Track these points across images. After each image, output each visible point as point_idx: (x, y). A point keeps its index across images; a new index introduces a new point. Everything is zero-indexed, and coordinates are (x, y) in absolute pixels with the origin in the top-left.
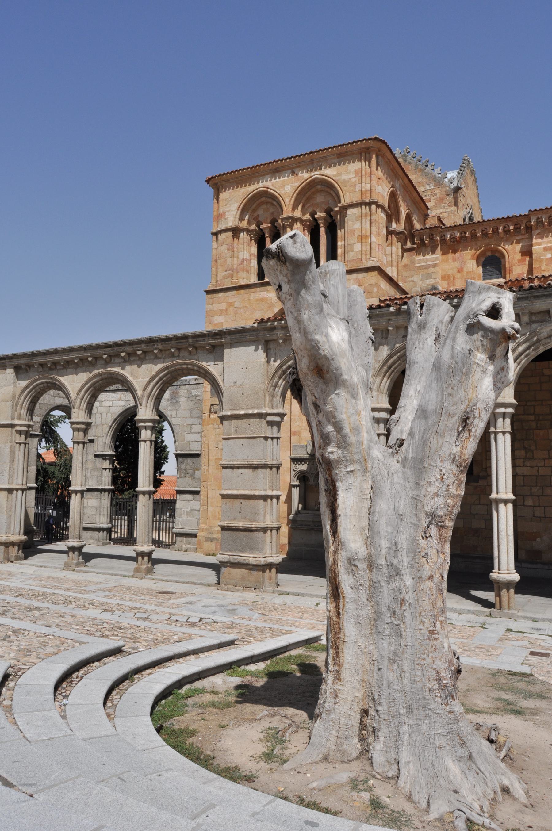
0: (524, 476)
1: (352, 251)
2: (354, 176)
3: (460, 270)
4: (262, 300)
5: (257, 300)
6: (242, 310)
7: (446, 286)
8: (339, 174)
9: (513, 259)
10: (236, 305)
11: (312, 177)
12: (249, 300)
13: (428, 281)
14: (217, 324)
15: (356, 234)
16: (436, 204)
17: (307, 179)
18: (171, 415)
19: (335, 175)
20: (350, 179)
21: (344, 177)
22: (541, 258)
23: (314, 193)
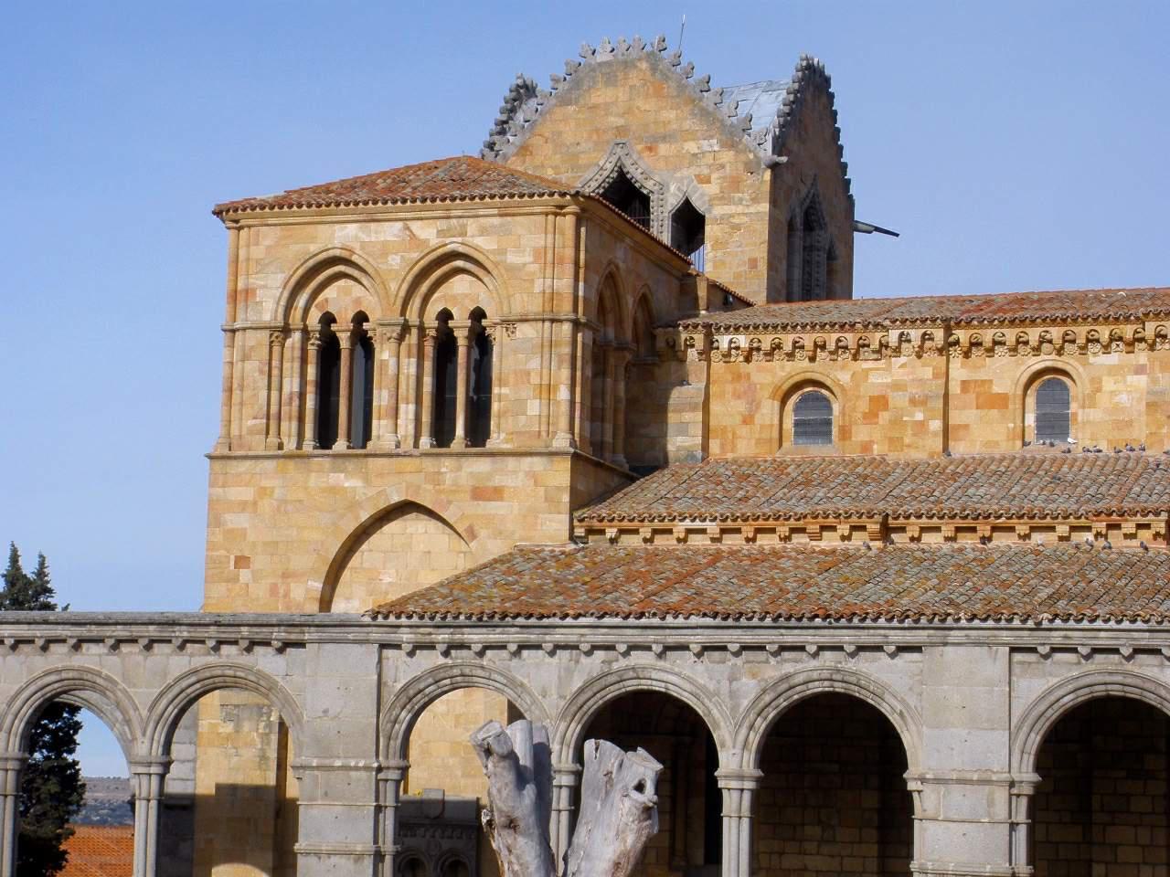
0: (817, 872)
1: (524, 413)
2: (531, 259)
3: (747, 420)
4: (334, 490)
6: (290, 507)
7: (718, 452)
8: (502, 251)
9: (854, 410)
10: (277, 494)
11: (446, 245)
12: (306, 488)
13: (679, 439)
15: (532, 381)
16: (722, 192)
17: (437, 249)
19: (493, 252)
20: (524, 265)
21: (512, 258)
22: (905, 419)
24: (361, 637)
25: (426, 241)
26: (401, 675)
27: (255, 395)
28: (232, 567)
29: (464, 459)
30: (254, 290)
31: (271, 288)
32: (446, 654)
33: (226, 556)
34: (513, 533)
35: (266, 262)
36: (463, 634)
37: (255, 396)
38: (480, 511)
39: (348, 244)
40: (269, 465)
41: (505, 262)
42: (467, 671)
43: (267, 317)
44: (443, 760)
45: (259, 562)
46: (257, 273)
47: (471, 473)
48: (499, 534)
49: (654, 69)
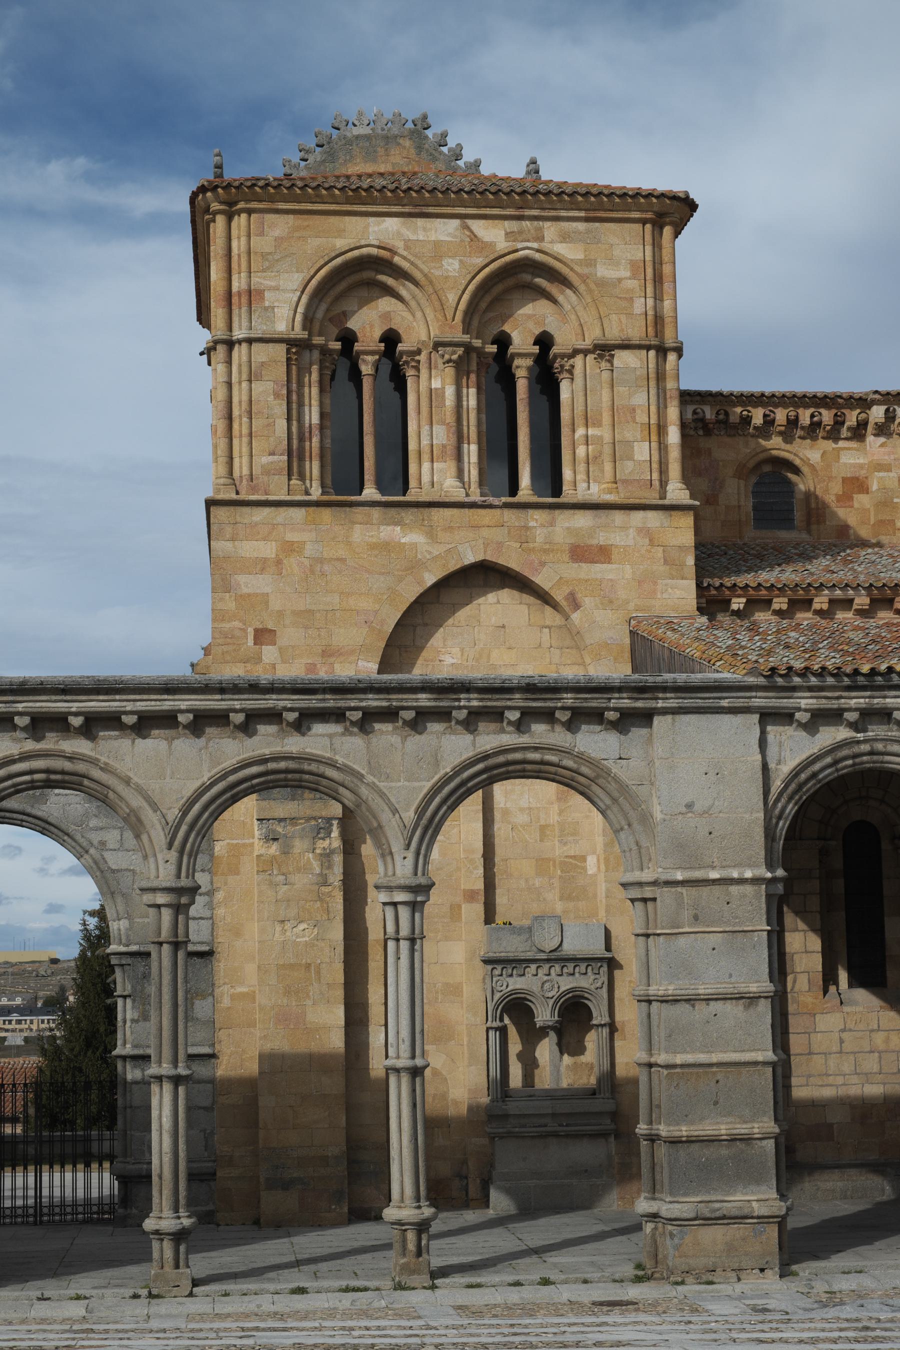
1: (631, 458)
2: (628, 274)
4: (386, 547)
5: (373, 547)
11: (517, 251)
12: (349, 544)
14: (249, 595)
15: (638, 419)
18: (103, 843)
19: (580, 262)
20: (620, 280)
21: (603, 271)
22: (895, 500)
23: (508, 291)
24: (740, 703)
25: (491, 245)
26: (786, 754)
27: (269, 425)
28: (250, 642)
29: (557, 512)
30: (261, 293)
31: (284, 291)
32: (855, 726)
33: (241, 629)
34: (627, 602)
35: (276, 257)
36: (885, 697)
37: (271, 425)
38: (582, 575)
39: (389, 241)
40: (298, 514)
41: (596, 275)
42: (880, 746)
43: (281, 327)
44: (527, 881)
45: (289, 635)
46: (263, 271)
47: (568, 528)
48: (609, 602)
49: (419, 148)
